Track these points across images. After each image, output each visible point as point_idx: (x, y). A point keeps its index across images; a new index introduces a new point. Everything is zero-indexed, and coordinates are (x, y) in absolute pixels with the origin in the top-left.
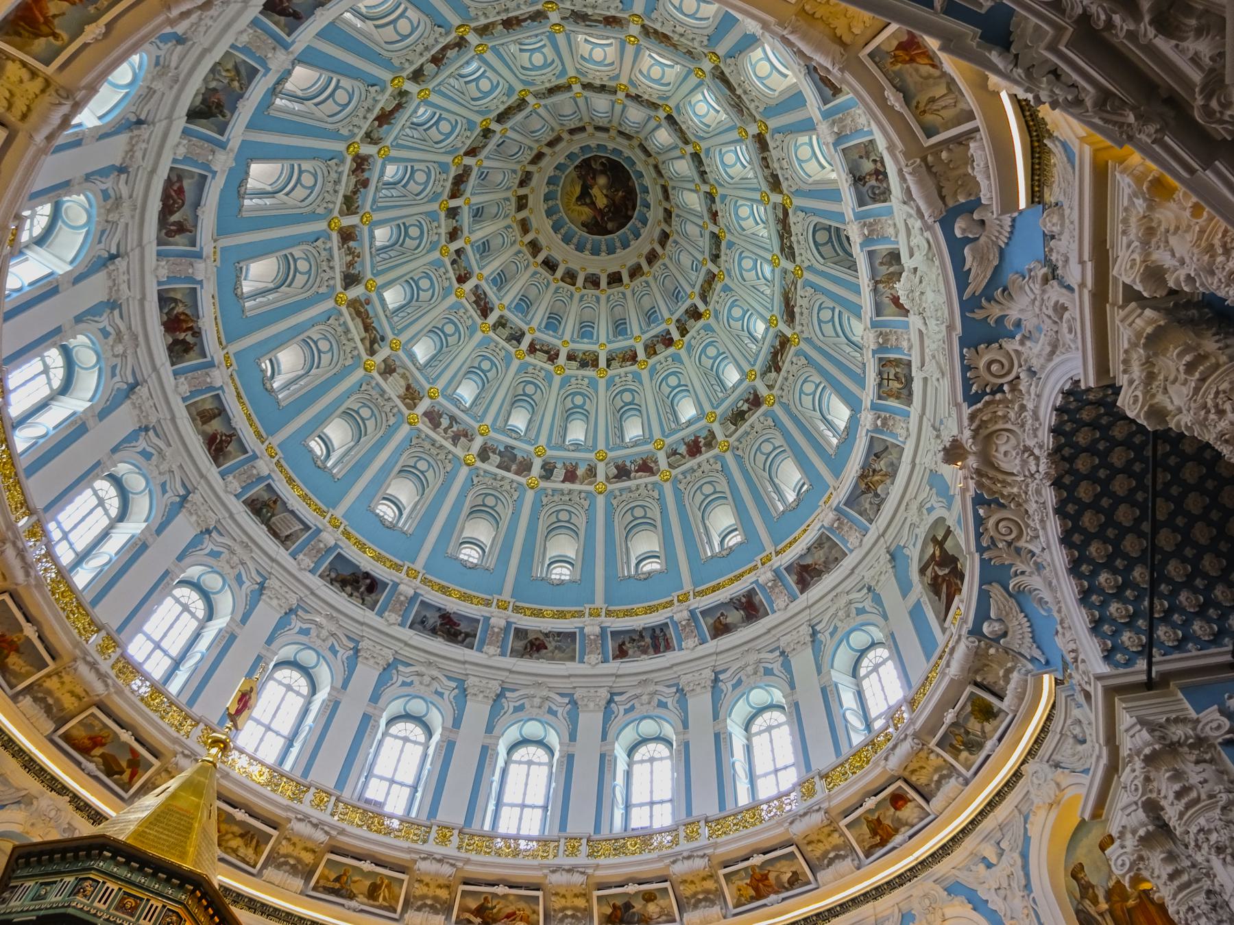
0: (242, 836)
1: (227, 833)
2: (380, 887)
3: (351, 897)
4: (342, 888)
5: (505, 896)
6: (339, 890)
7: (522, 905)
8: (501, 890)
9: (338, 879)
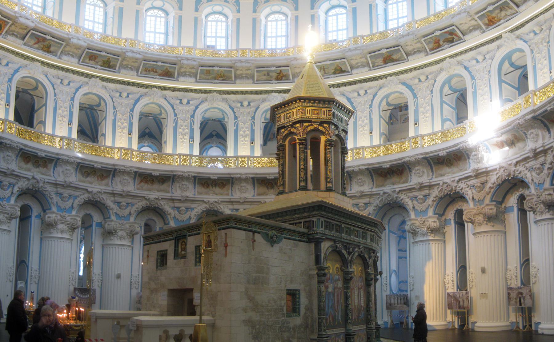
0: (501, 10)
1: (497, 15)
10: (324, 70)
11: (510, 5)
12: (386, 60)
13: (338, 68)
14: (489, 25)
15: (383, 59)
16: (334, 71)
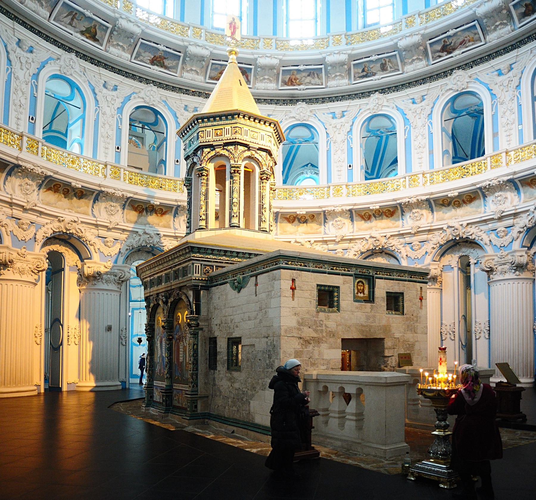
0: (309, 75)
2: (385, 64)
3: (374, 74)
4: (368, 73)
5: (455, 34)
6: (366, 75)
7: (467, 34)
8: (451, 32)
9: (363, 71)
10: (72, 19)
11: (321, 75)
12: (155, 60)
13: (93, 30)
14: (286, 84)
15: (152, 57)
16: (84, 29)
